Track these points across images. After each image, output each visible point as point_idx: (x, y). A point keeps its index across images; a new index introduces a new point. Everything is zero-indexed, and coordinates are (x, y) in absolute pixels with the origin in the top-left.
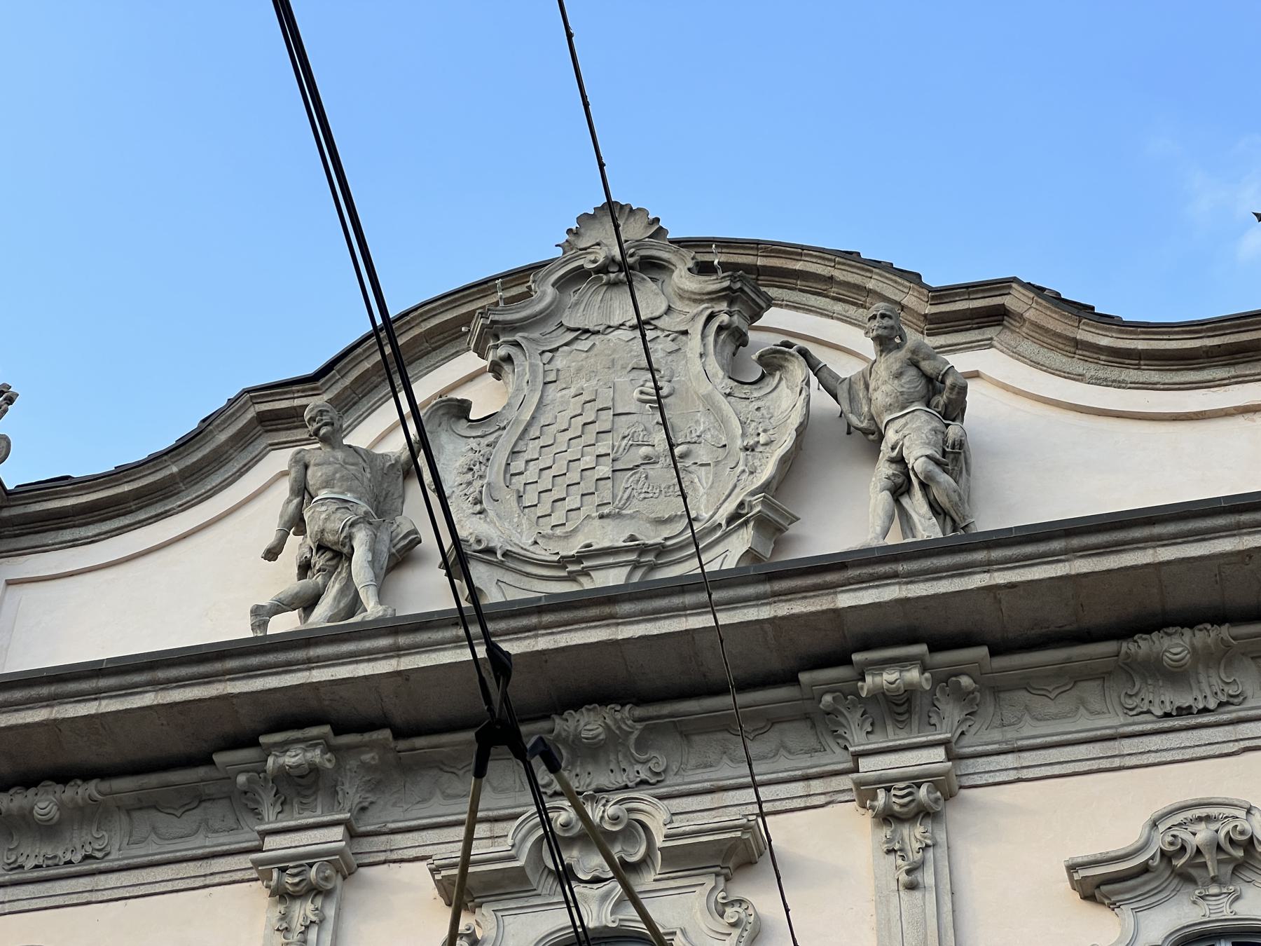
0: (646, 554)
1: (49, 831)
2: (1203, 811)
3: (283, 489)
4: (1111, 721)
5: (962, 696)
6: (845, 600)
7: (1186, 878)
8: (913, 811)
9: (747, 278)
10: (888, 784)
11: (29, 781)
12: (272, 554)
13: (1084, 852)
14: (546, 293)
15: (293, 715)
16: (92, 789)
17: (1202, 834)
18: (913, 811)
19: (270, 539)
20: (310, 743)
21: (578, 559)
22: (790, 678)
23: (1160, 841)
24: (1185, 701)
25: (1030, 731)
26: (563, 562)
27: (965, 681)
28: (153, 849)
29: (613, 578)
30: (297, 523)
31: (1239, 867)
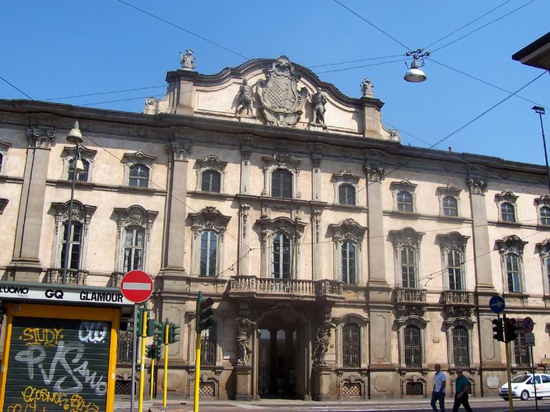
9: (300, 72)
24: (346, 155)
30: (240, 96)
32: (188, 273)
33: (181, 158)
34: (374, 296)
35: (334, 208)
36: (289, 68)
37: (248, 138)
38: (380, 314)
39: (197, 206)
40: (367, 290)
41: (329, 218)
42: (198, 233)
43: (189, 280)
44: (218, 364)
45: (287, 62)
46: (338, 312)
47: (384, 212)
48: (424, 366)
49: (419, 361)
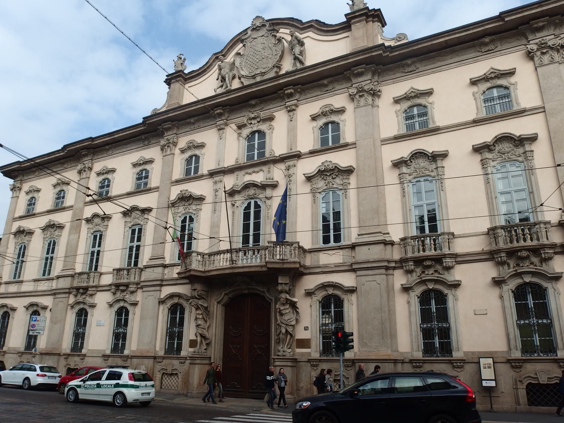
0: (263, 74)
1: (193, 124)
2: (326, 106)
3: (218, 70)
4: (319, 93)
5: (299, 92)
6: (281, 81)
7: (325, 115)
8: (291, 111)
10: (289, 106)
11: (190, 117)
12: (217, 79)
13: (311, 114)
14: (249, 32)
15: (217, 106)
16: (197, 118)
17: (327, 109)
18: (291, 111)
19: (217, 77)
20: (219, 109)
21: (254, 75)
22: (276, 93)
23: (321, 111)
25: (309, 96)
26: (252, 76)
27: (299, 90)
28: (206, 124)
29: (258, 79)
31: (331, 113)
32: (167, 262)
33: (168, 152)
34: (363, 254)
35: (313, 153)
36: (264, 26)
37: (219, 111)
38: (370, 278)
39: (175, 192)
40: (353, 247)
41: (310, 165)
42: (178, 218)
43: (165, 266)
44: (183, 353)
45: (261, 21)
46: (311, 282)
47: (382, 141)
48: (456, 355)
49: (447, 348)
